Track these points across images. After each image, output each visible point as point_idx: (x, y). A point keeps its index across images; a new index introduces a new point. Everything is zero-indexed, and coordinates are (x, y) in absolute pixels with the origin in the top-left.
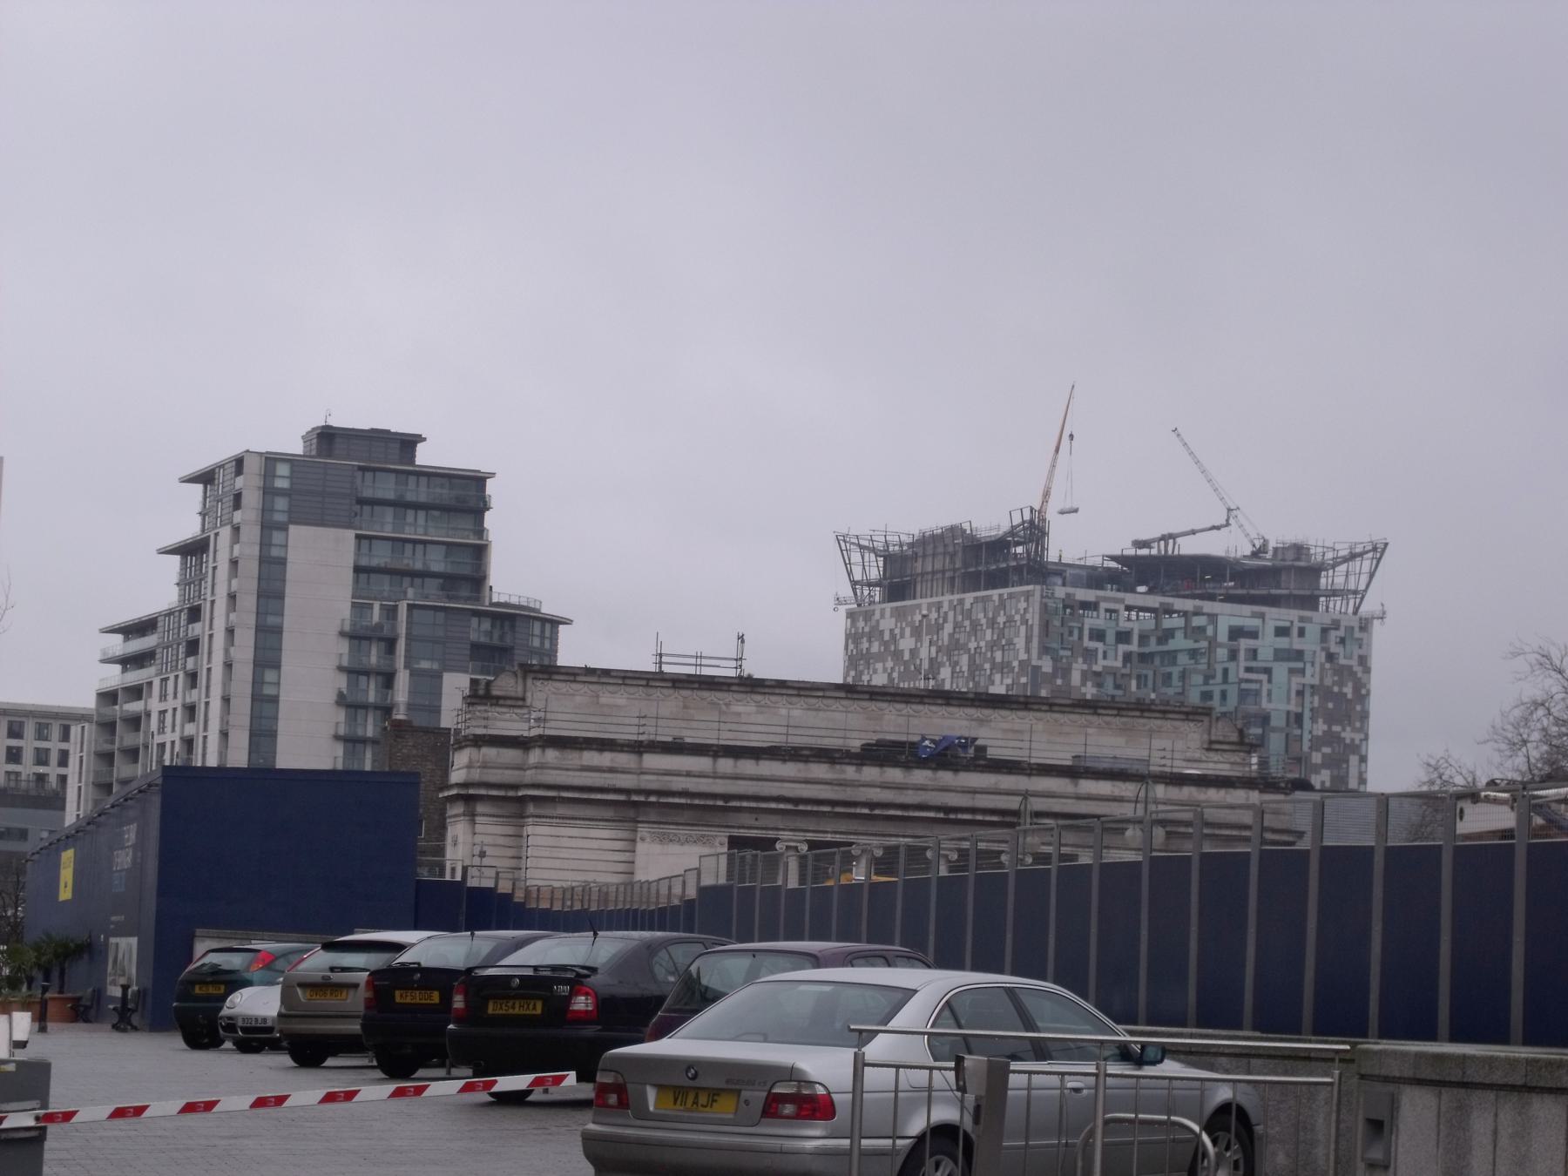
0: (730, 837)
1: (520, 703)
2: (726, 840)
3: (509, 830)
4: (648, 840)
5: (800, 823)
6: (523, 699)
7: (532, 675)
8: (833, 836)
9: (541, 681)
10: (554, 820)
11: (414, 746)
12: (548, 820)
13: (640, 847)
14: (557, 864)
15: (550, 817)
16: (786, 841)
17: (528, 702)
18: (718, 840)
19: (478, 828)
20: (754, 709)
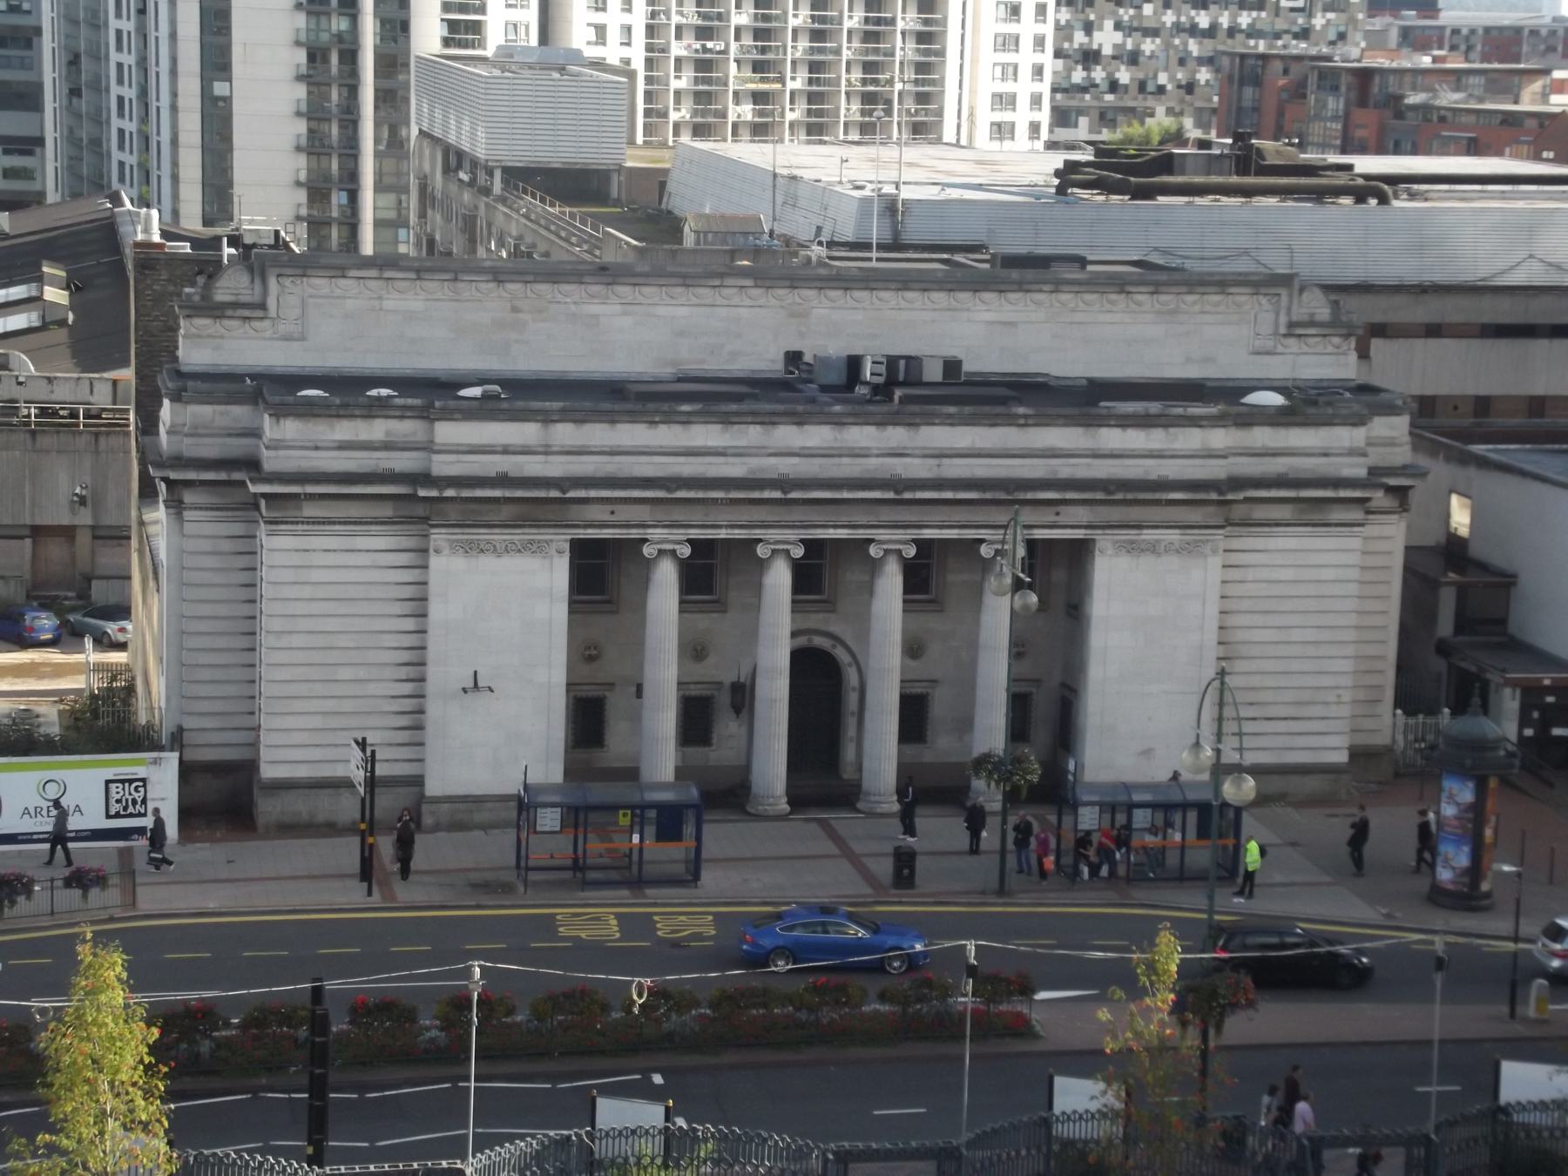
0: (572, 541)
1: (259, 313)
2: (567, 546)
3: (238, 529)
4: (446, 552)
5: (678, 514)
6: (262, 306)
7: (278, 271)
8: (730, 531)
9: (291, 279)
10: (300, 527)
11: (169, 280)
13: (435, 562)
14: (307, 592)
15: (292, 523)
16: (658, 543)
17: (272, 310)
18: (554, 546)
19: (189, 528)
20: (618, 308)
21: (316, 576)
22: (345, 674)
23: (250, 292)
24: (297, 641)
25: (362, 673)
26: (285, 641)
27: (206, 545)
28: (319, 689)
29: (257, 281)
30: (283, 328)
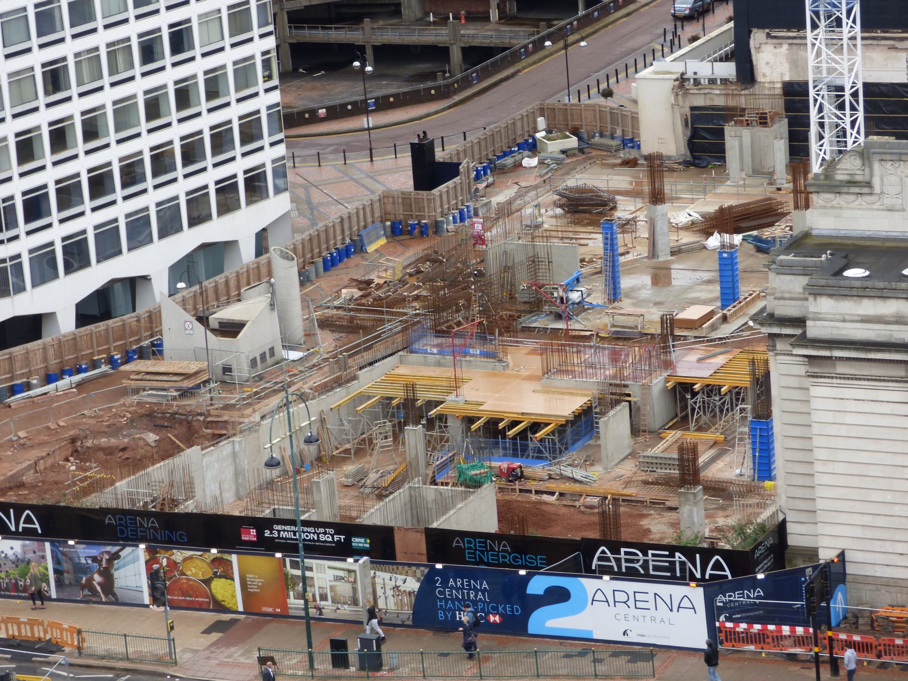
6: (869, 184)
7: (878, 157)
10: (835, 381)
12: (827, 380)
14: (843, 431)
15: (829, 377)
17: (877, 189)
21: (849, 419)
22: (876, 496)
23: (861, 172)
24: (839, 468)
25: (889, 497)
26: (830, 468)
27: (794, 382)
28: (858, 507)
29: (867, 163)
30: (888, 201)
